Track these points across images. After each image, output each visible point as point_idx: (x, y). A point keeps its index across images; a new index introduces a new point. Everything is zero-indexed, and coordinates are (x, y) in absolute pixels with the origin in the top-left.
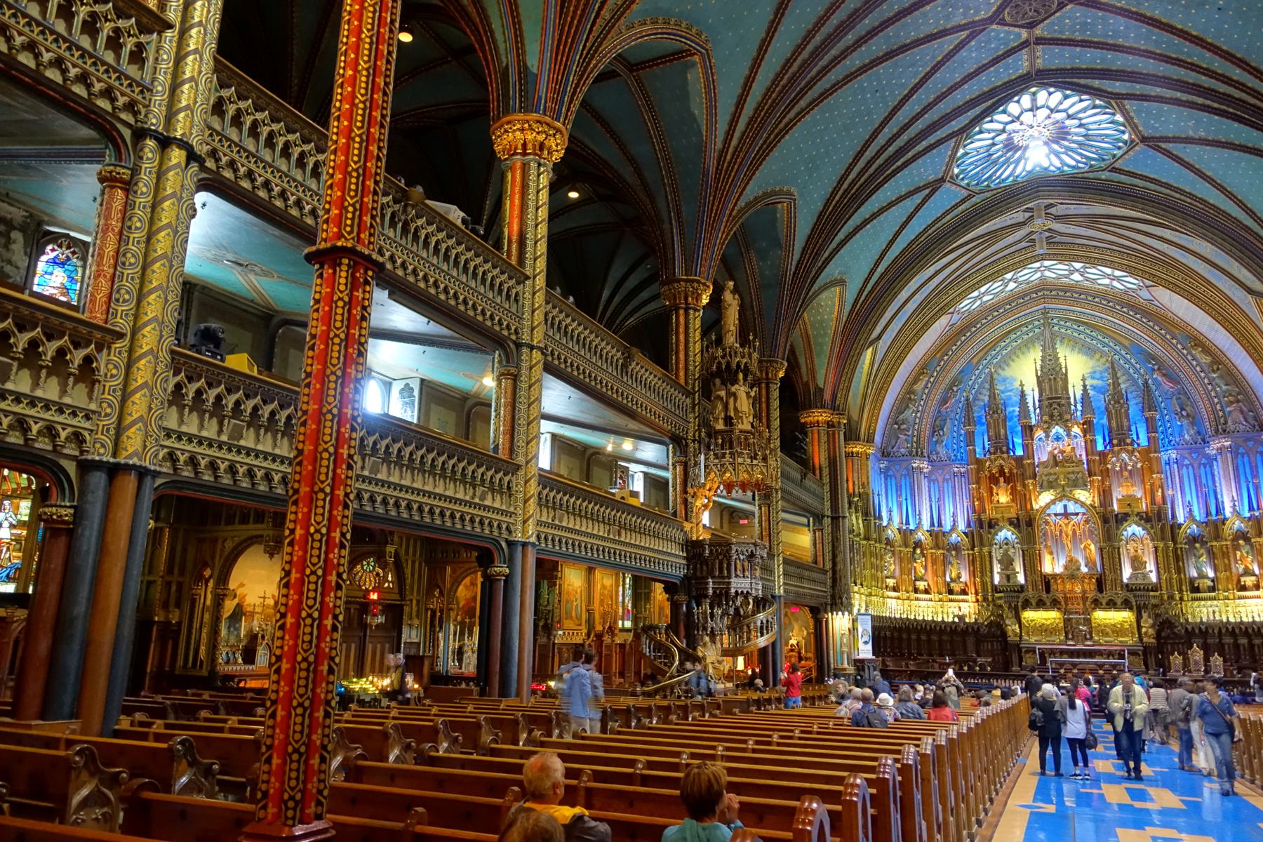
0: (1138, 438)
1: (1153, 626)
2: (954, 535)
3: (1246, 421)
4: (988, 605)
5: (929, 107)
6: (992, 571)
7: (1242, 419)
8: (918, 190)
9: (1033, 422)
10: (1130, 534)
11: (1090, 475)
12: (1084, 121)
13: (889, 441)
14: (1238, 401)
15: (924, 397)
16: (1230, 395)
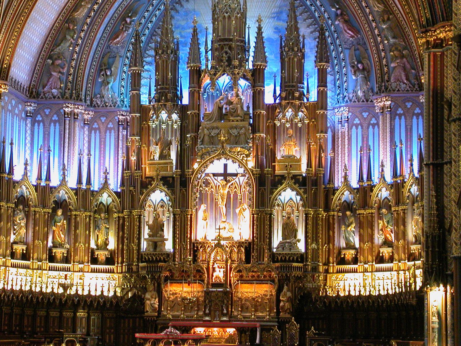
0: (308, 92)
1: (289, 300)
2: (105, 195)
3: (407, 79)
6: (139, 239)
7: (404, 78)
11: (254, 131)
13: (40, 79)
14: (403, 56)
15: (86, 27)
16: (396, 49)
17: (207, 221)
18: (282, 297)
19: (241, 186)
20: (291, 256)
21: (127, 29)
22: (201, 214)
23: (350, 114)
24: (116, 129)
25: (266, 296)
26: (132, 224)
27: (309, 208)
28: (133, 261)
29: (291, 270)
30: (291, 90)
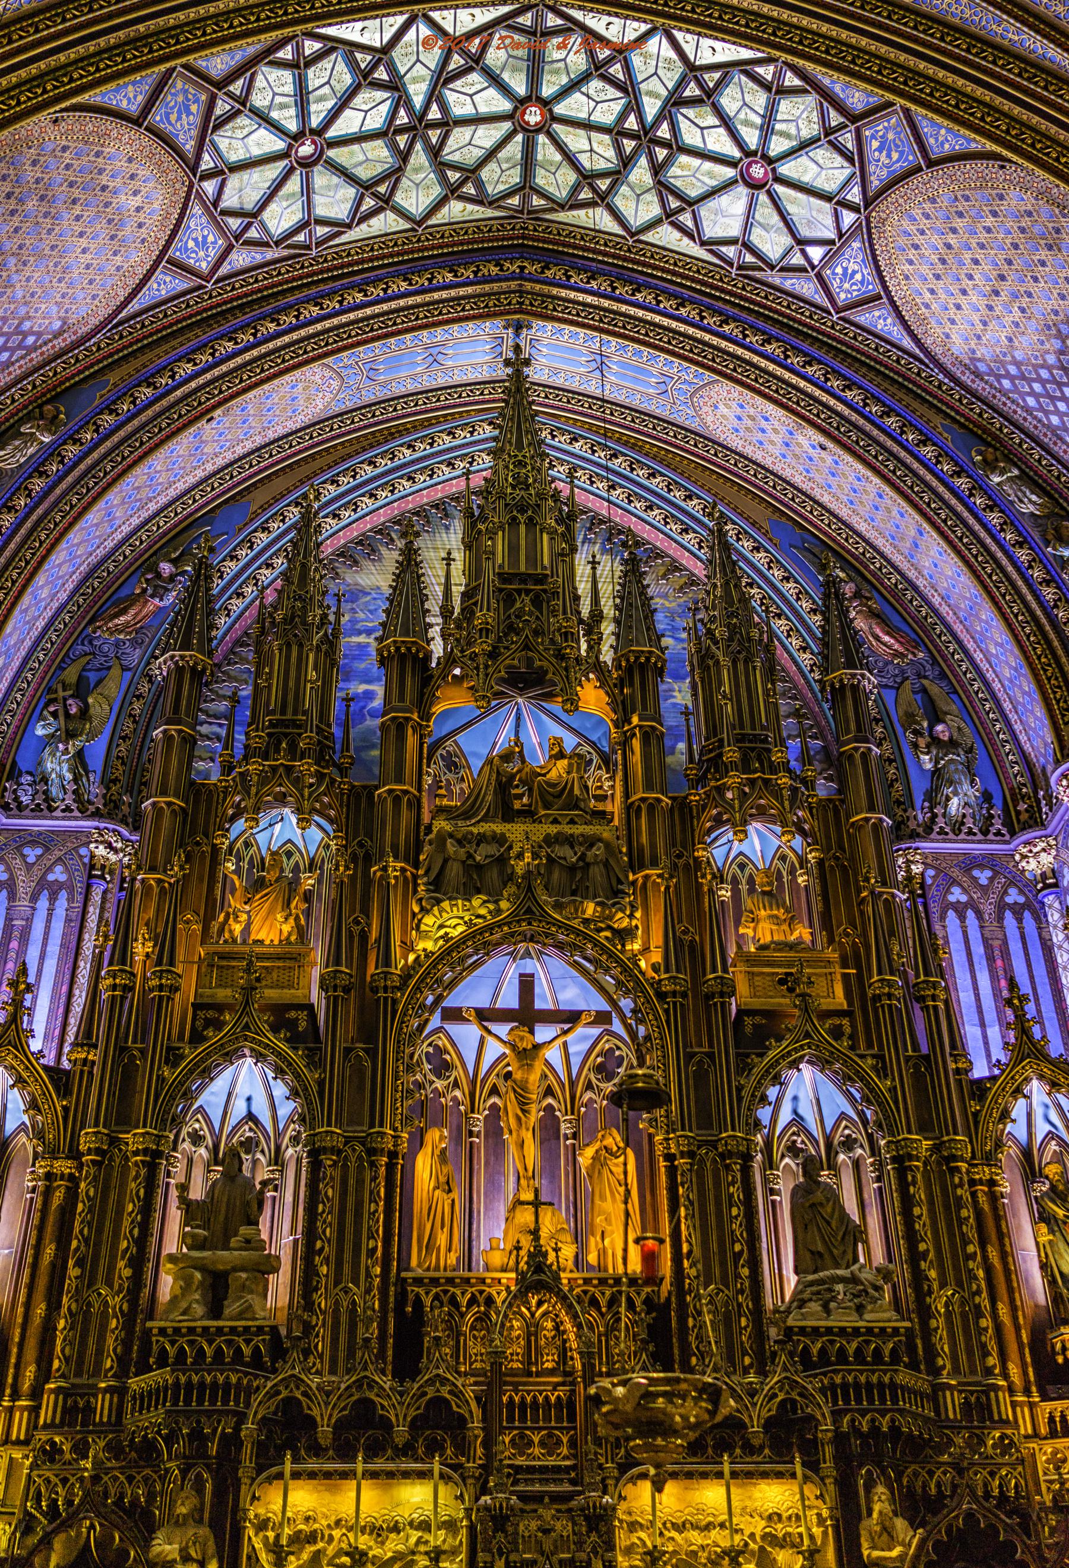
4: (81, 1450)
6: (137, 1263)
9: (437, 648)
10: (785, 1116)
17: (455, 1195)
18: (874, 1547)
19: (573, 1084)
20: (868, 1342)
21: (159, 592)
22: (424, 1167)
23: (931, 872)
24: (79, 887)
25: (781, 1543)
26: (113, 1196)
27: (909, 1132)
28: (97, 1371)
29: (895, 1401)
30: (753, 749)
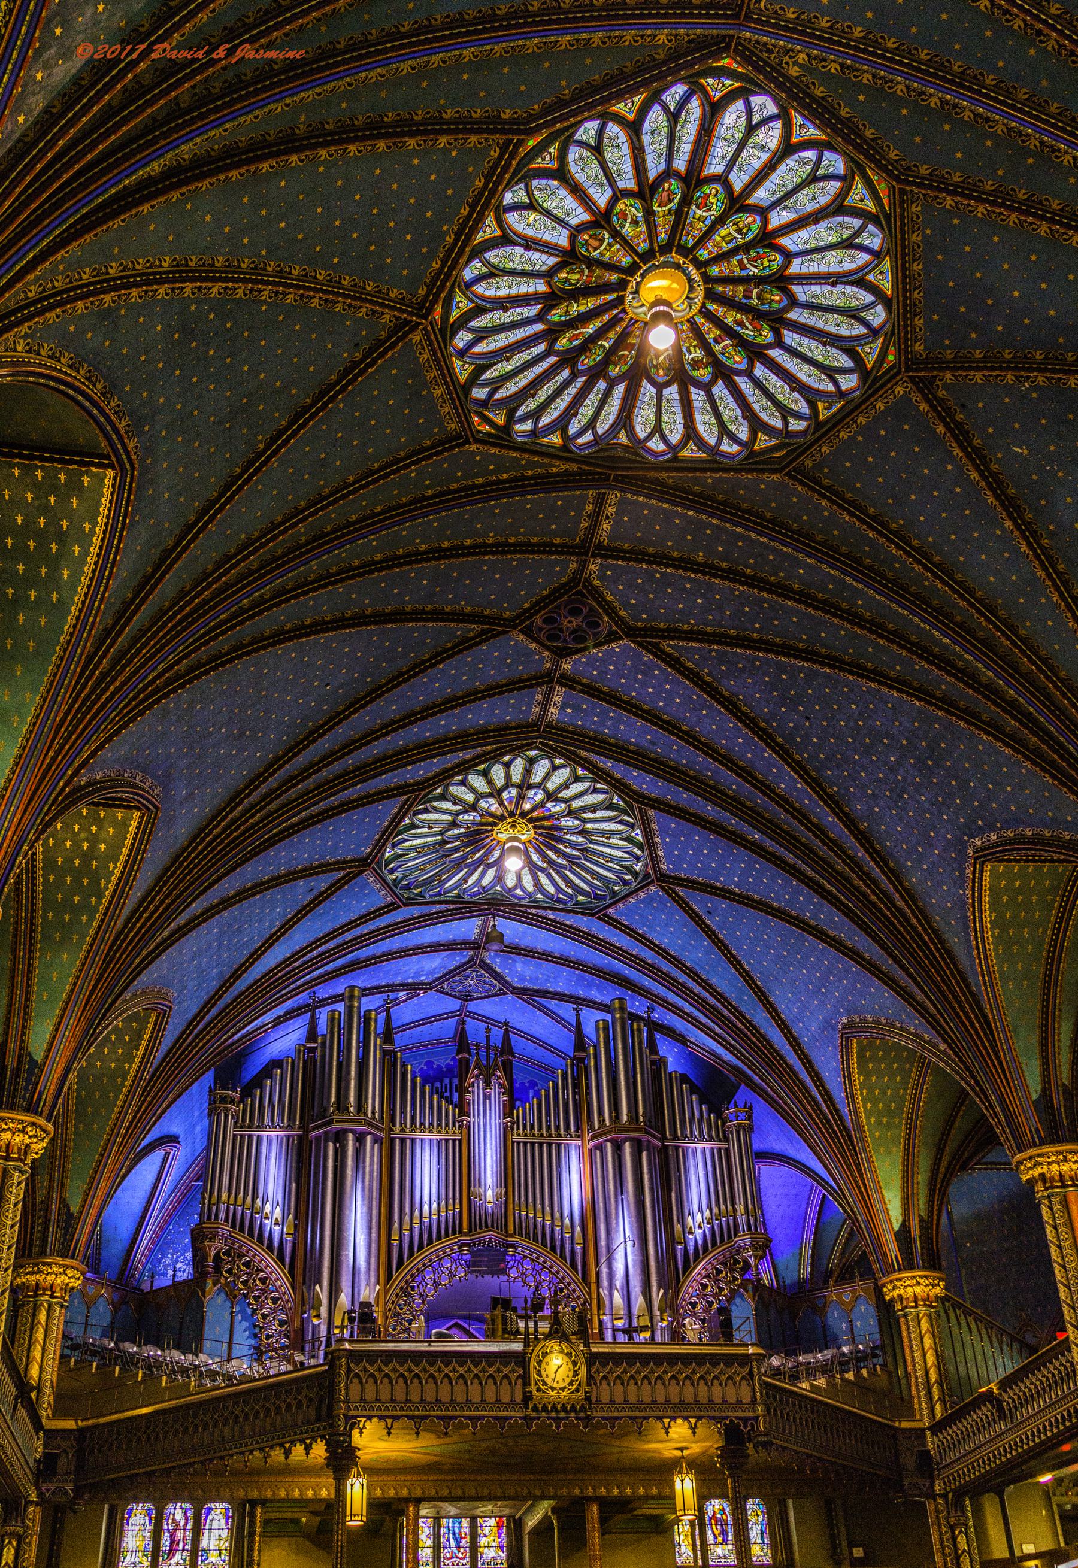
5: (410, 718)
8: (325, 868)
12: (588, 826)
